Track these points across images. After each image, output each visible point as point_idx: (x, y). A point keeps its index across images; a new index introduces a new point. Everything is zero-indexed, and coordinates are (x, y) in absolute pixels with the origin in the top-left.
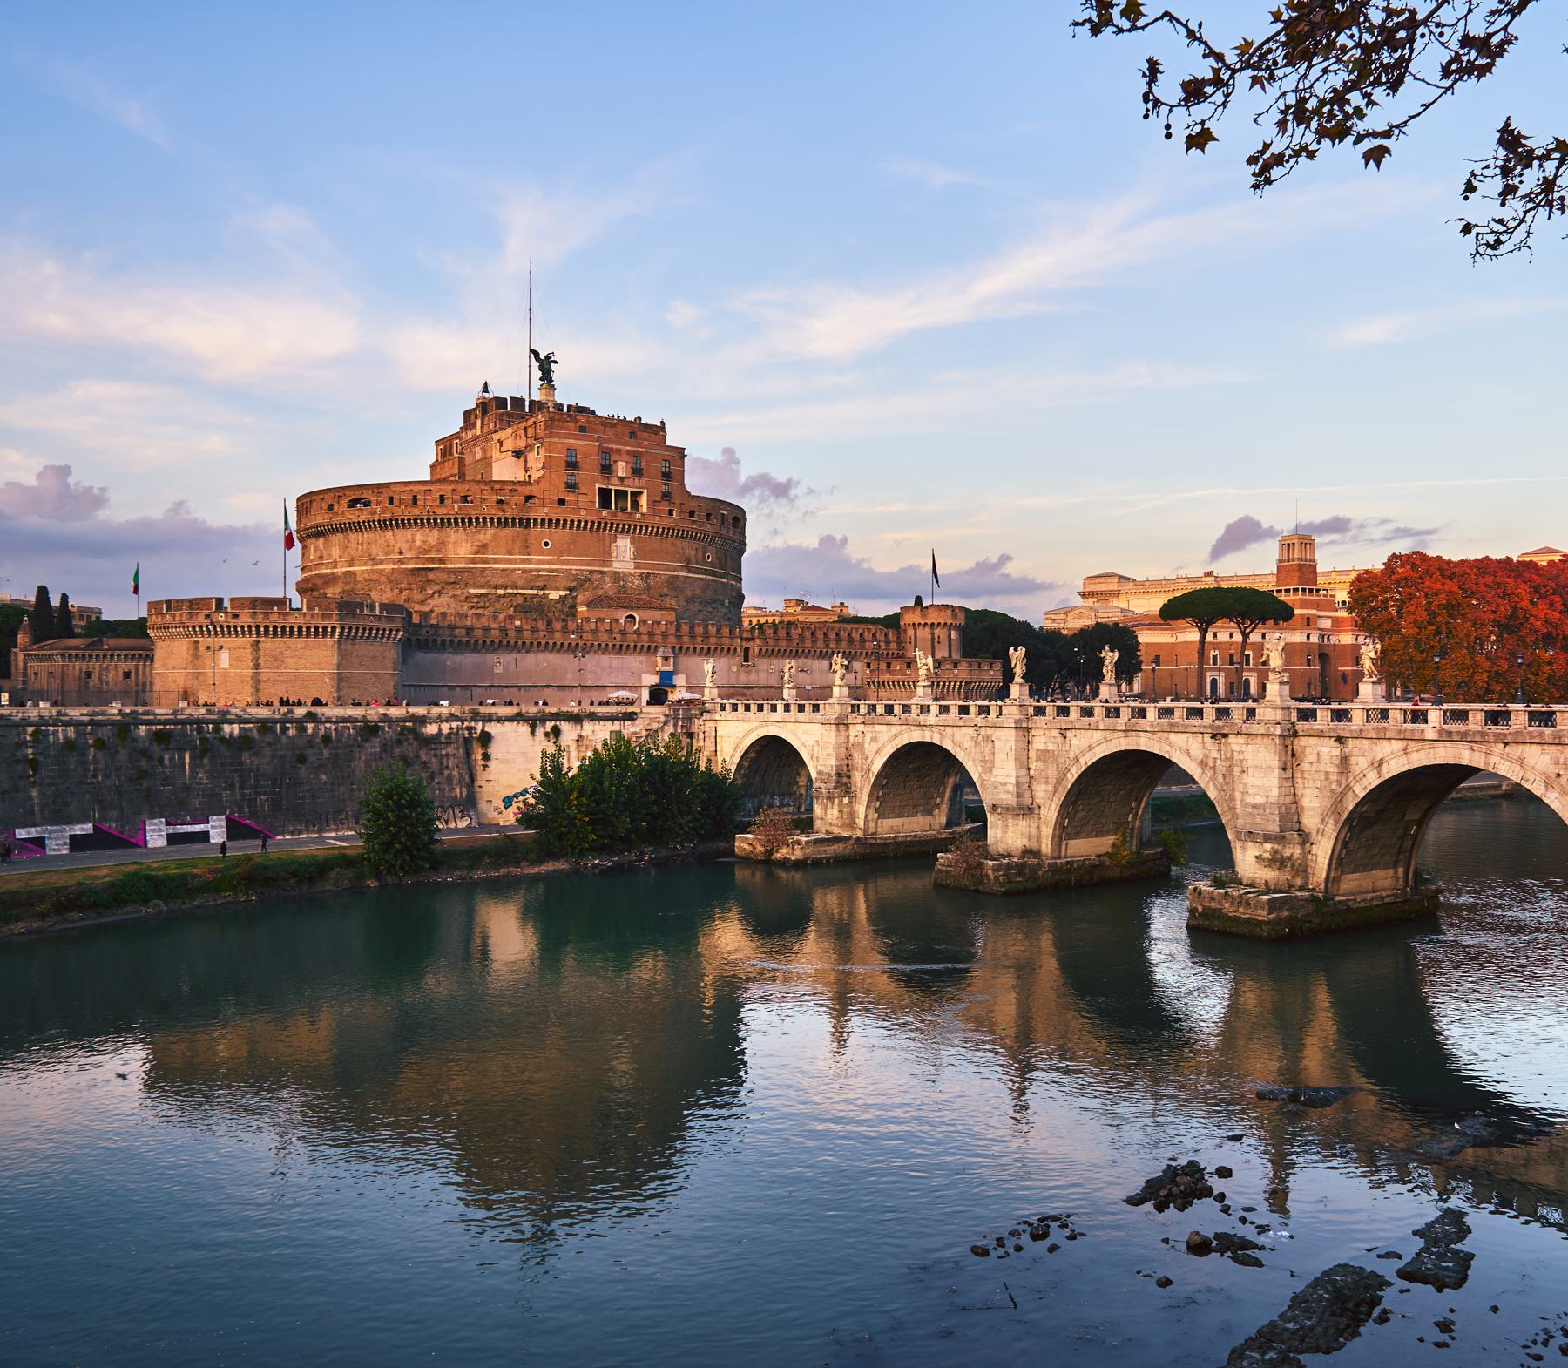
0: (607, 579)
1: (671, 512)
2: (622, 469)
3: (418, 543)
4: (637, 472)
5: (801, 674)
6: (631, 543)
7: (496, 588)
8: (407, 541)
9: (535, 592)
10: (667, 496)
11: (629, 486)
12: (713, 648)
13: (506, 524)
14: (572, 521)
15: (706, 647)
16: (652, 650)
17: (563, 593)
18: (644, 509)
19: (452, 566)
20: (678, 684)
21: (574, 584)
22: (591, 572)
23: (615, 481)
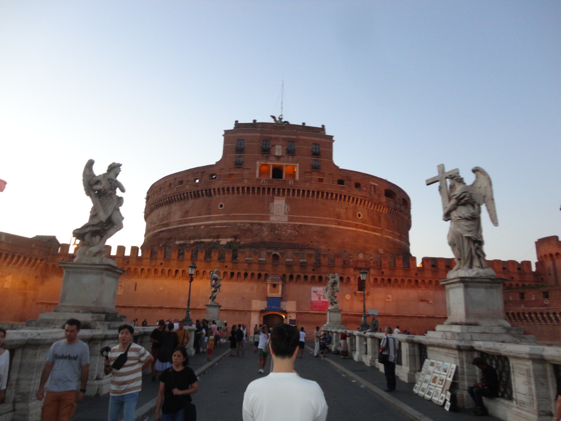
0: (265, 229)
1: (321, 180)
2: (278, 150)
3: (160, 216)
4: (290, 152)
5: (422, 304)
6: (286, 203)
7: (190, 239)
9: (210, 240)
12: (324, 277)
13: (199, 196)
14: (238, 188)
15: (317, 276)
16: (263, 277)
17: (229, 240)
18: (297, 178)
19: (171, 227)
21: (238, 233)
22: (252, 224)
23: (272, 158)
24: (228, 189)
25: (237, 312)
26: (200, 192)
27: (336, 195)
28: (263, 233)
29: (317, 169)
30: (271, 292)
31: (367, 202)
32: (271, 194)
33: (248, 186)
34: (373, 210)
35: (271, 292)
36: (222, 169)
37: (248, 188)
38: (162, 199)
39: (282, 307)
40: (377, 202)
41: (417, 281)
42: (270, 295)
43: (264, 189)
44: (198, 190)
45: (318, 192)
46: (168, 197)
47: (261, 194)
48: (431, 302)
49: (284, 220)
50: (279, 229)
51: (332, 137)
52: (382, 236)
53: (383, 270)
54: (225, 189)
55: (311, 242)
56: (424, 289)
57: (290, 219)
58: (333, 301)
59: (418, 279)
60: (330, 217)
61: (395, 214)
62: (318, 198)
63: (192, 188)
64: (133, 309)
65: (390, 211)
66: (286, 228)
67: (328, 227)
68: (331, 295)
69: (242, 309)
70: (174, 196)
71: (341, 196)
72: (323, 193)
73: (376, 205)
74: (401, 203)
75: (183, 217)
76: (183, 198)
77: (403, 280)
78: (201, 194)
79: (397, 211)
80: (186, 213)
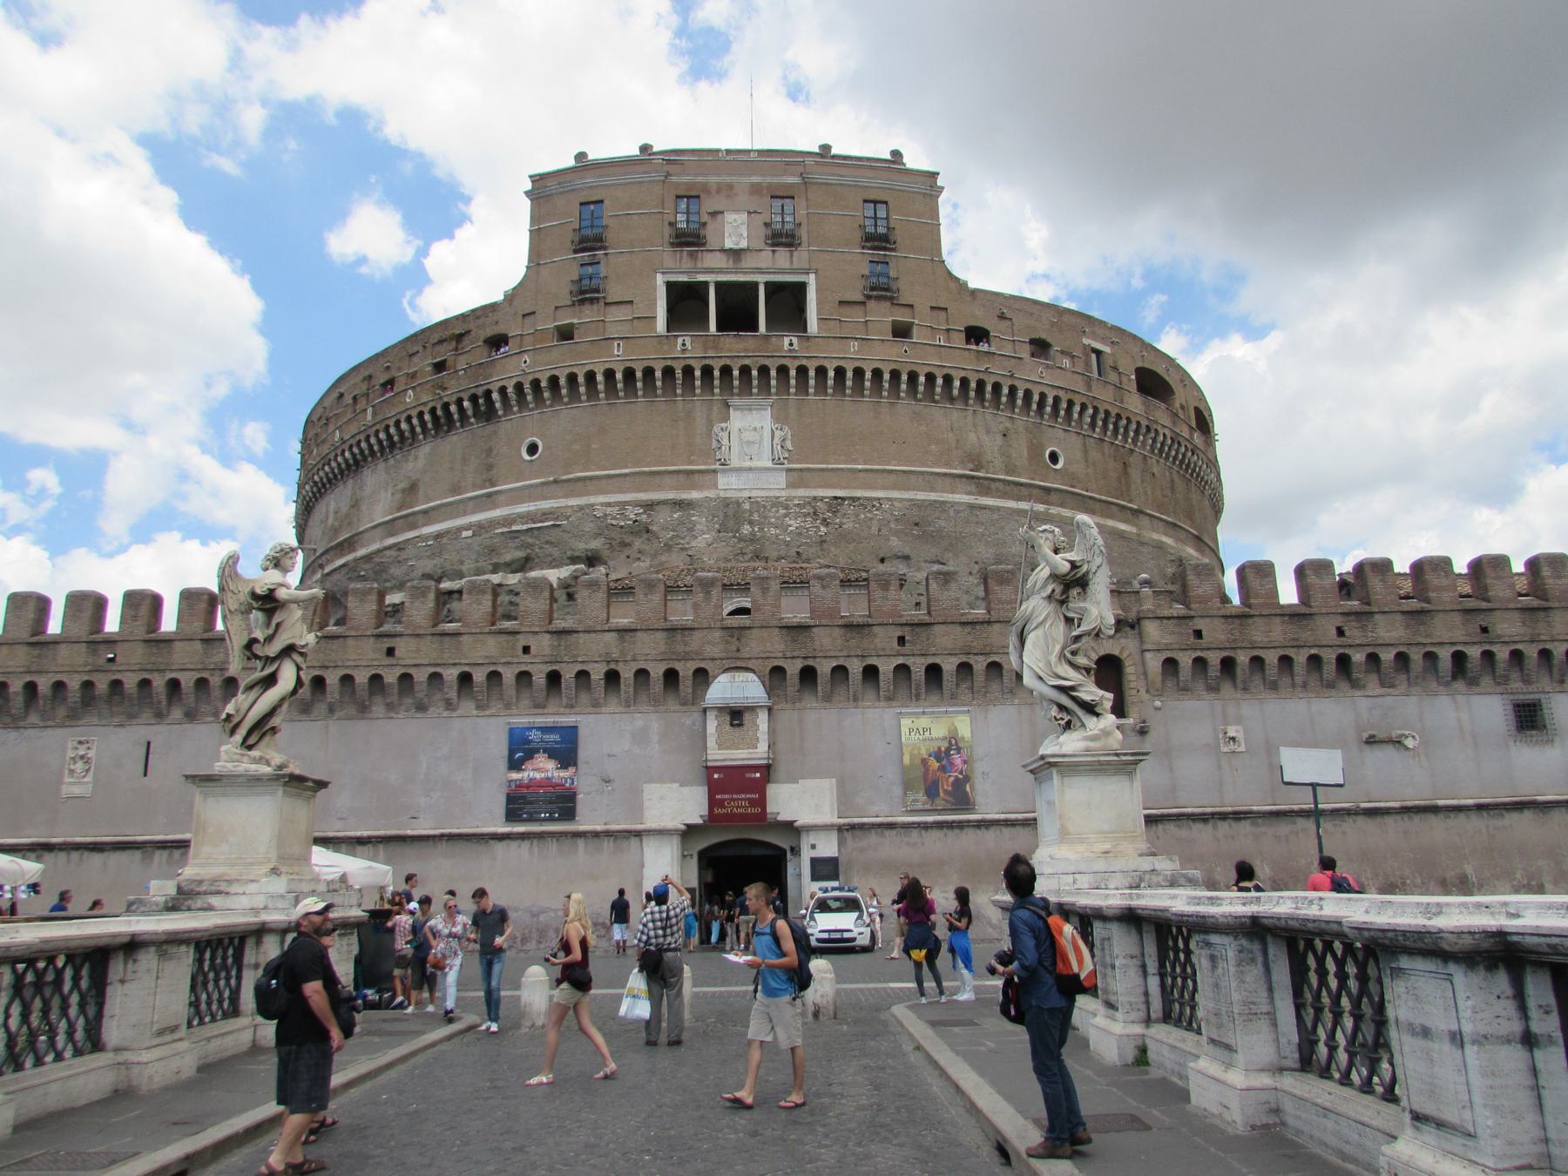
0: (700, 521)
1: (901, 331)
2: (735, 230)
6: (776, 418)
8: (322, 522)
10: (881, 290)
11: (760, 271)
12: (949, 665)
14: (590, 376)
15: (918, 666)
16: (686, 684)
17: (565, 572)
19: (361, 552)
20: (803, 819)
21: (595, 544)
22: (649, 506)
24: (554, 381)
25: (581, 842)
26: (453, 408)
27: (965, 382)
28: (696, 537)
29: (887, 290)
30: (721, 746)
31: (1077, 408)
32: (717, 391)
33: (628, 364)
34: (1102, 440)
35: (721, 746)
36: (524, 316)
37: (629, 374)
38: (332, 456)
39: (769, 810)
40: (1113, 412)
41: (1343, 662)
42: (718, 755)
43: (688, 371)
44: (445, 400)
45: (895, 375)
46: (346, 446)
47: (679, 391)
48: (1409, 743)
49: (776, 485)
50: (756, 517)
51: (934, 175)
52: (1138, 535)
53: (1200, 624)
54: (544, 384)
55: (882, 560)
56: (1379, 691)
57: (798, 478)
58: (1074, 699)
59: (1346, 651)
60: (947, 465)
61: (1175, 458)
62: (898, 398)
63: (425, 399)
64: (137, 855)
65: (1159, 445)
66: (782, 511)
67: (943, 502)
68: (1053, 658)
69: (599, 828)
70: (368, 437)
71: (981, 384)
72: (913, 377)
73: (1112, 420)
74: (1194, 424)
75: (399, 509)
76: (396, 438)
77: (1286, 661)
78: (456, 417)
79: (1183, 449)
80: (413, 488)
